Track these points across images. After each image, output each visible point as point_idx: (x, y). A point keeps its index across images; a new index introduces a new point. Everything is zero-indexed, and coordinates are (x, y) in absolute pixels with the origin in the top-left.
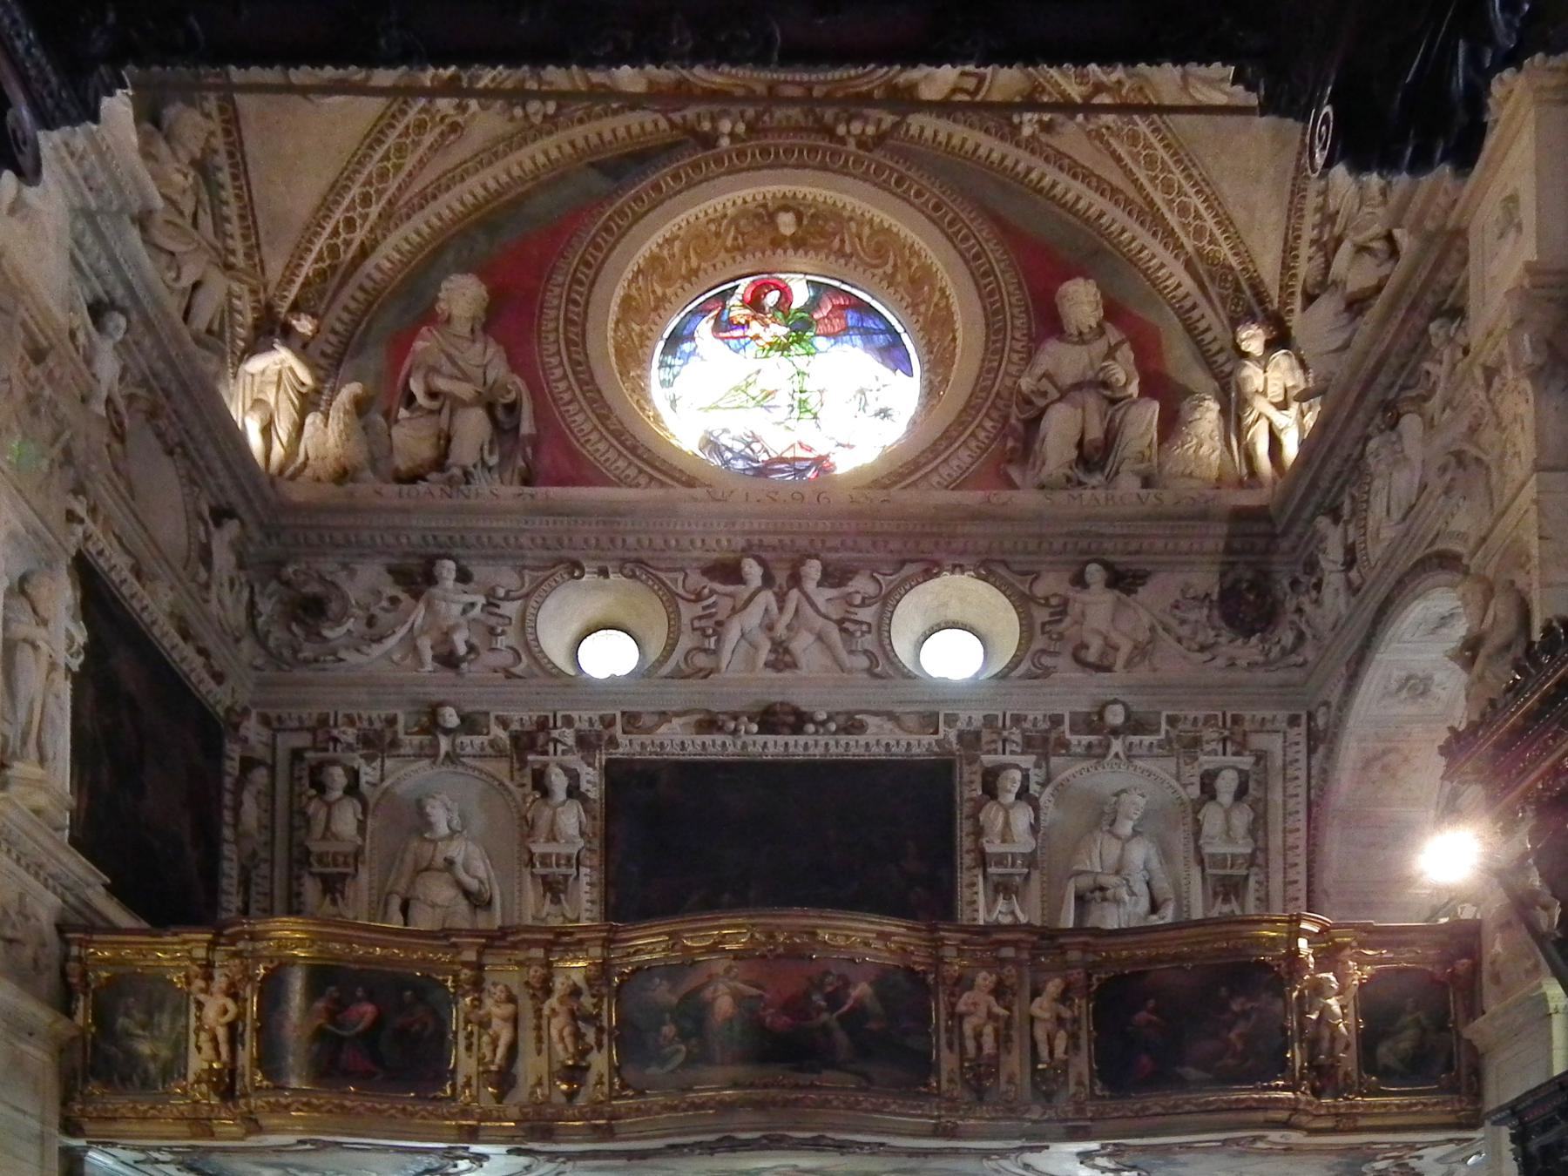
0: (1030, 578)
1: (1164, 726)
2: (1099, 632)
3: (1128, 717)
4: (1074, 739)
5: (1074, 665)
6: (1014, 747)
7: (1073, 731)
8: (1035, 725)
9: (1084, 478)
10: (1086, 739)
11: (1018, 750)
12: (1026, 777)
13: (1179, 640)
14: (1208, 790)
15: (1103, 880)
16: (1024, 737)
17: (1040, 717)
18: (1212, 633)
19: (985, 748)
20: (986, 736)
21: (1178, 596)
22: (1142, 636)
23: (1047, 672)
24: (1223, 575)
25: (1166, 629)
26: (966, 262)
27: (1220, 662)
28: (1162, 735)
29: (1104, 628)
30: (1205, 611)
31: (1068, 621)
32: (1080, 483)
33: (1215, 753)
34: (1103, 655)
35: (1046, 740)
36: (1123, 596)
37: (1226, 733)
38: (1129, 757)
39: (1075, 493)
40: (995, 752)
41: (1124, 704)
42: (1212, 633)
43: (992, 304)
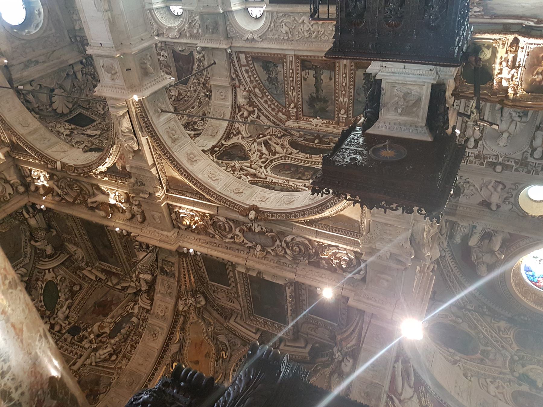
1: (485, 163)
2: (497, 192)
3: (495, 167)
4: (513, 164)
5: (506, 185)
6: (532, 164)
7: (513, 166)
8: (523, 170)
10: (509, 163)
12: (532, 155)
13: (474, 186)
14: (476, 142)
15: (518, 119)
16: (527, 167)
17: (521, 172)
18: (464, 186)
20: (539, 169)
21: (471, 197)
22: (484, 189)
23: (515, 184)
24: (458, 200)
25: (477, 189)
27: (464, 178)
28: (486, 160)
30: (465, 192)
31: (505, 196)
33: (472, 153)
34: (497, 186)
35: (521, 165)
36: (487, 200)
37: (467, 158)
38: (498, 156)
40: (539, 164)
41: (495, 171)
42: (464, 186)
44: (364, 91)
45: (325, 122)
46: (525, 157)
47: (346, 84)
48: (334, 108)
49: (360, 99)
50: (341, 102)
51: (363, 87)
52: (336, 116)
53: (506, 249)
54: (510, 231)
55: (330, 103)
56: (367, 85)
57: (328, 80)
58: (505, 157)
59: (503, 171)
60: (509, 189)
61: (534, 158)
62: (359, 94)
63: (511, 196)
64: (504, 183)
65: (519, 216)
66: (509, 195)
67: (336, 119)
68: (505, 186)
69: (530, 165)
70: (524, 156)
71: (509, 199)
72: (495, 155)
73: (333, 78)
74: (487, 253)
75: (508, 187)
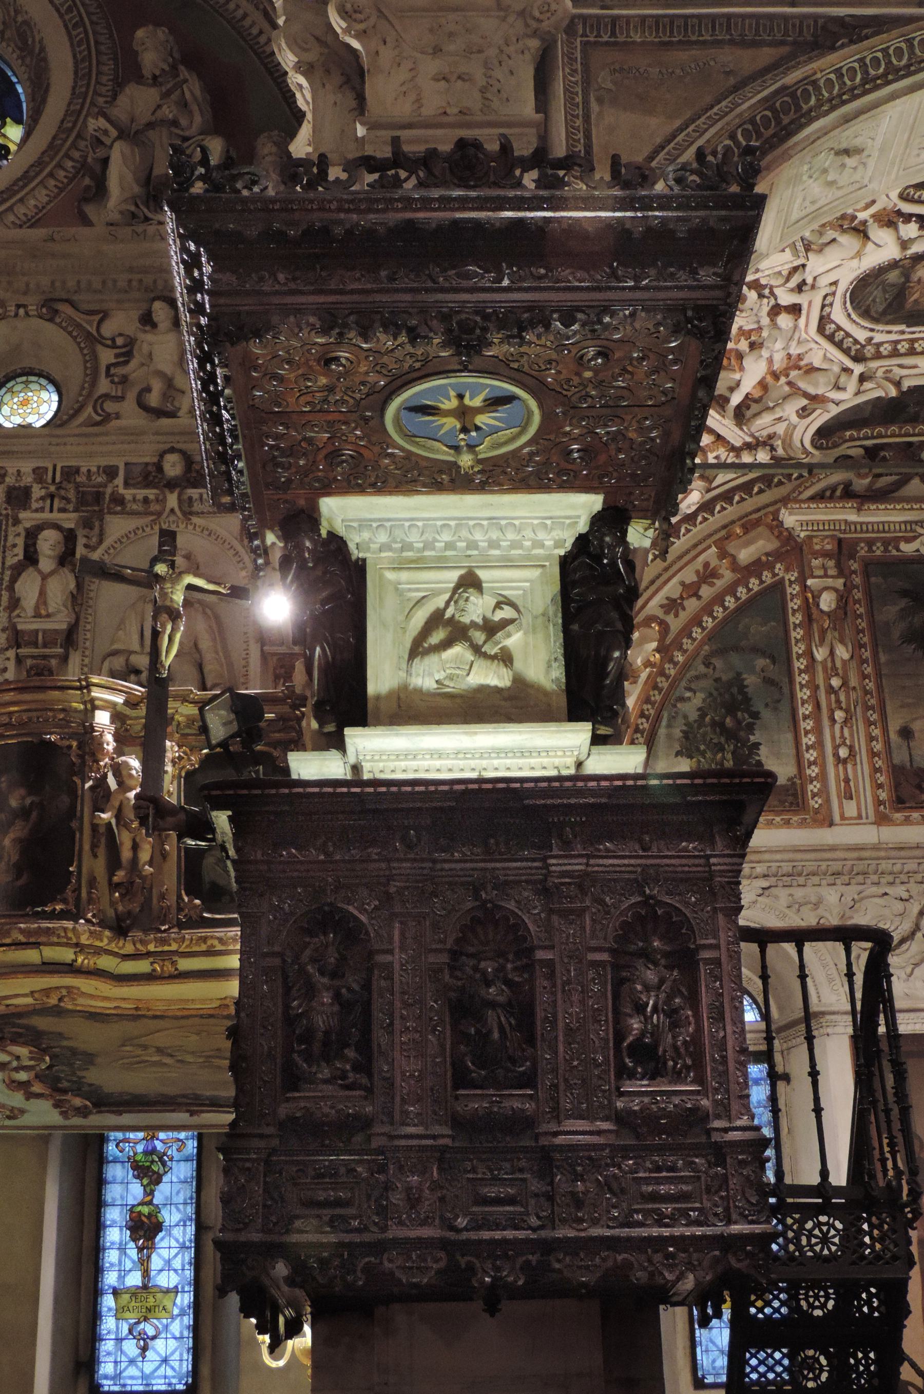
0: (97, 318)
2: (160, 374)
4: (128, 493)
7: (127, 485)
9: (150, 215)
10: (141, 493)
11: (71, 507)
17: (94, 469)
19: (35, 505)
20: (37, 492)
26: (61, 16)
29: (168, 369)
31: (133, 363)
32: (147, 219)
34: (165, 396)
38: (185, 514)
39: (140, 228)
40: (42, 509)
43: (80, 52)
44: (747, 700)
45: (904, 547)
46: (91, 529)
47: (833, 721)
48: (871, 613)
49: (761, 662)
50: (842, 641)
51: (756, 715)
52: (857, 580)
53: (89, 160)
54: (85, 231)
55: (896, 633)
56: (739, 722)
57: (916, 726)
58: (159, 514)
59: (155, 460)
60: (122, 398)
61: (57, 527)
62: (769, 682)
63: (113, 371)
64: (144, 414)
65: (67, 301)
66: (120, 371)
67: (855, 566)
68: (142, 405)
69: (68, 501)
70: (96, 530)
71: (117, 356)
72: (197, 514)
73: (893, 736)
74: (150, 125)
75: (129, 406)
